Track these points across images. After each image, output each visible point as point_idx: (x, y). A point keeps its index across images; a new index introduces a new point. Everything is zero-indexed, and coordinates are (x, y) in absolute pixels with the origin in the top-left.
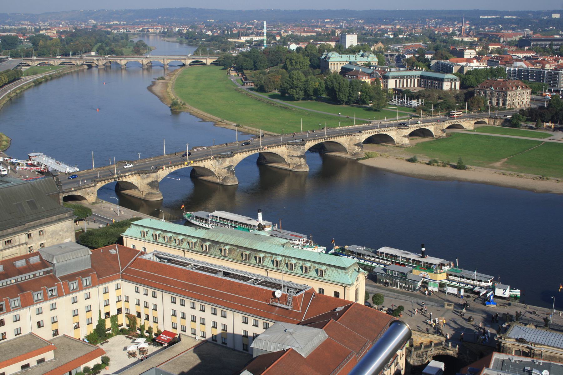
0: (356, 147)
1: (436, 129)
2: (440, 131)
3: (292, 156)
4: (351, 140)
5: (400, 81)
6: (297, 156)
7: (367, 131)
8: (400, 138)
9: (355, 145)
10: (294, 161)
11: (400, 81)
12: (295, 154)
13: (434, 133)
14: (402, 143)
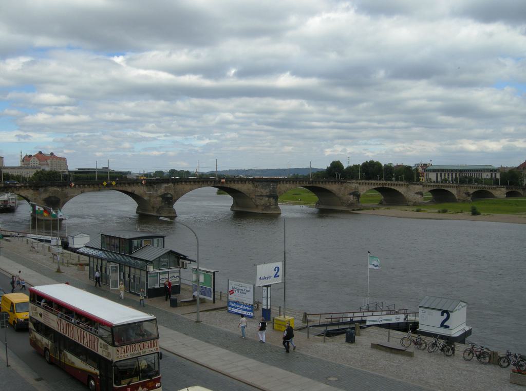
0: (352, 196)
1: (459, 192)
2: (464, 195)
3: (261, 196)
4: (346, 188)
5: (441, 174)
6: (267, 196)
7: (367, 181)
8: (413, 195)
9: (350, 194)
10: (263, 202)
11: (441, 174)
12: (264, 193)
13: (457, 198)
14: (414, 201)
